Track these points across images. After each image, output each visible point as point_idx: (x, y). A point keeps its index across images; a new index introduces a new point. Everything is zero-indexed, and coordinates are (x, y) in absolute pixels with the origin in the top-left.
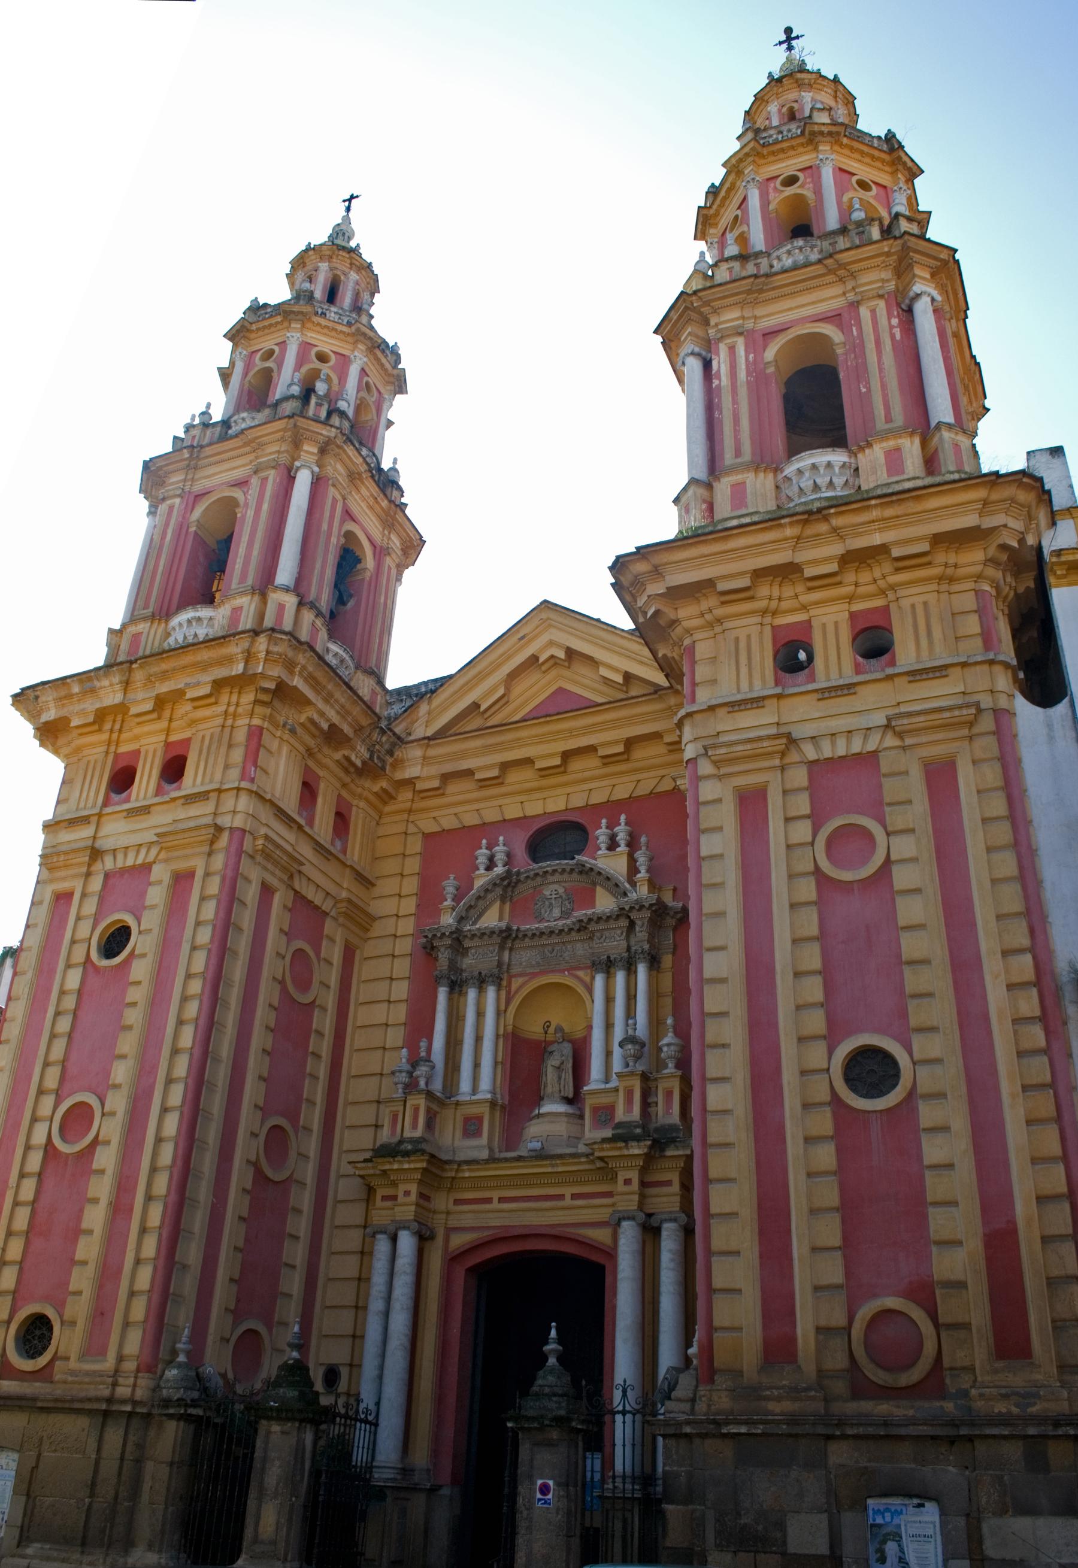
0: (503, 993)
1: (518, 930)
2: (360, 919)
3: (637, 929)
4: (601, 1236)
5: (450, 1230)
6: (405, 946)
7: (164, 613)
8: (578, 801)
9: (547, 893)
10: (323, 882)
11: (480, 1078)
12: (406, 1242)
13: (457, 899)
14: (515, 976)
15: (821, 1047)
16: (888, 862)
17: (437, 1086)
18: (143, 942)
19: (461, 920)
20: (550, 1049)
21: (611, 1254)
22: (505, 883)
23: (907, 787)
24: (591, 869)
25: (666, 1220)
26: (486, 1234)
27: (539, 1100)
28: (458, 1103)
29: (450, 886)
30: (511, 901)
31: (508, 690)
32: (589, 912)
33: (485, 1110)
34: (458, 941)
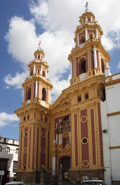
6: (54, 130)
8: (68, 114)
11: (61, 142)
13: (58, 125)
15: (81, 139)
16: (87, 120)
17: (57, 143)
18: (28, 134)
19: (58, 128)
23: (89, 113)
27: (66, 144)
29: (57, 124)
31: (61, 103)
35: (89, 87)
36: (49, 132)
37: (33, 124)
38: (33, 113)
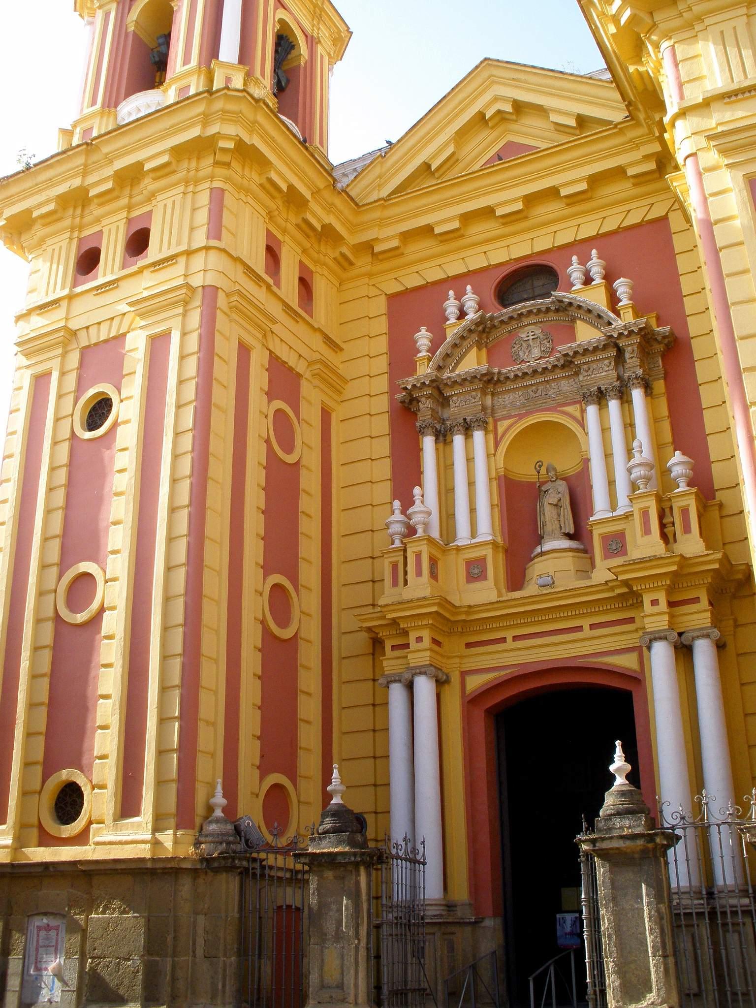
0: (491, 436)
1: (499, 373)
2: (333, 381)
3: (627, 355)
4: (628, 662)
5: (464, 674)
6: (382, 404)
7: (112, 102)
9: (524, 335)
10: (296, 345)
11: (479, 522)
12: (424, 687)
13: (432, 350)
14: (500, 420)
17: (435, 534)
18: (127, 410)
19: (440, 368)
20: (544, 488)
21: (639, 679)
22: (480, 328)
24: (570, 304)
25: (698, 637)
26: (503, 673)
28: (458, 549)
29: (423, 338)
30: (486, 346)
32: (574, 345)
33: (488, 552)
34: (440, 391)
36: (326, 416)
37: (197, 302)
38: (204, 199)
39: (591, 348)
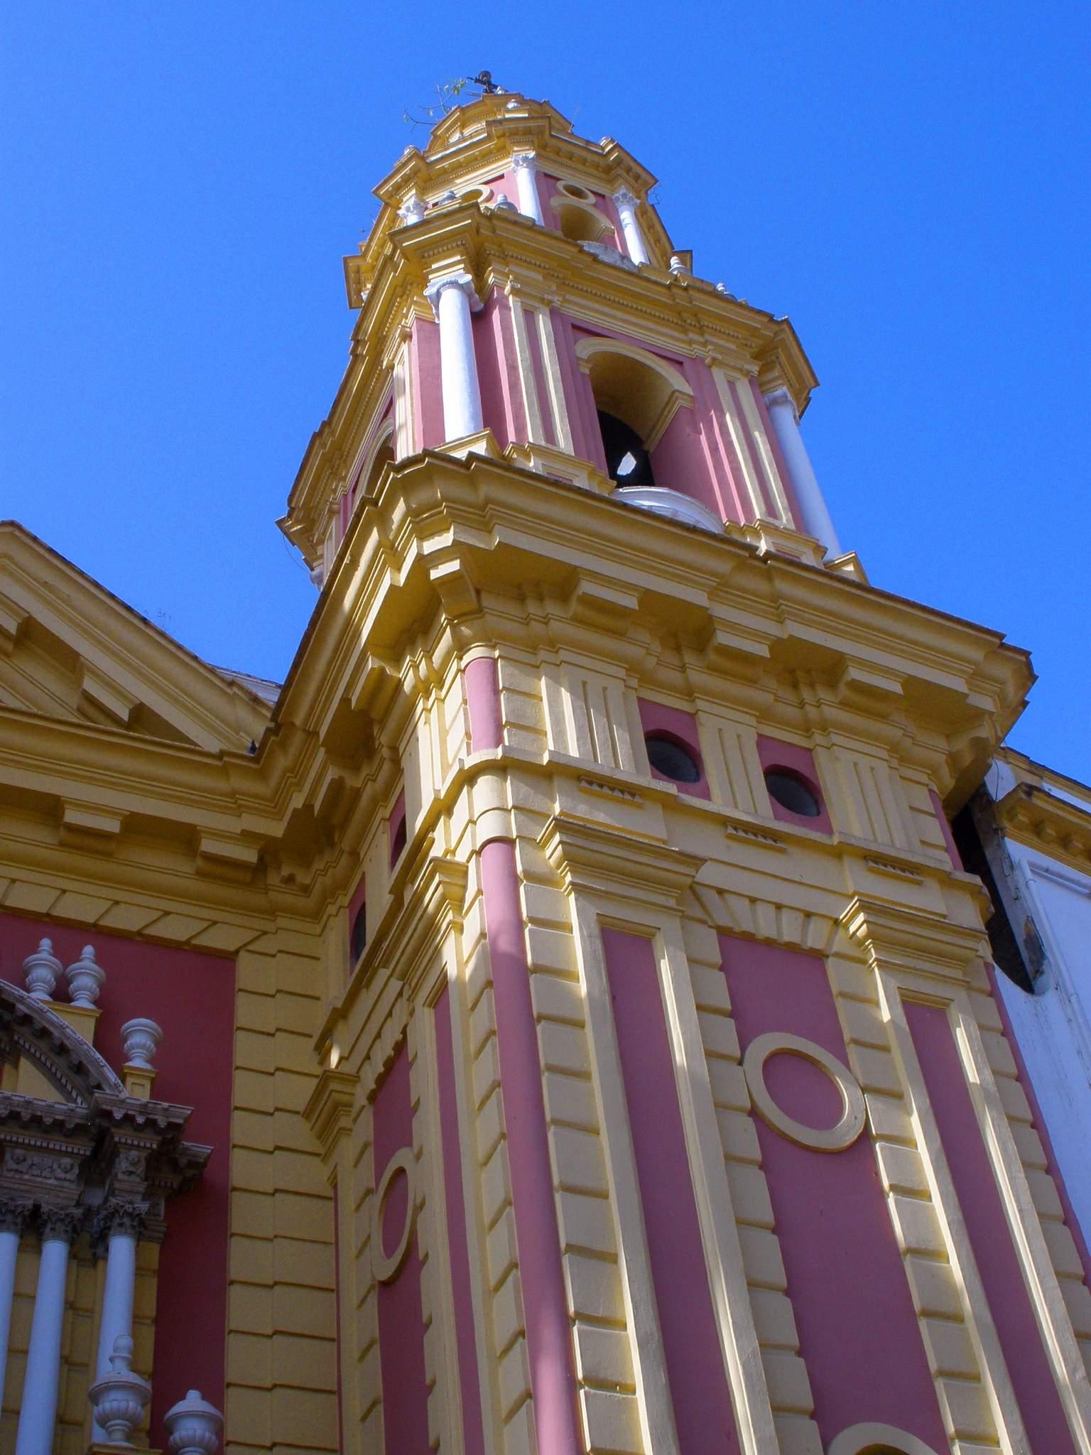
3: (122, 1164)
24: (27, 1020)
35: (869, 700)
39: (48, 1120)
